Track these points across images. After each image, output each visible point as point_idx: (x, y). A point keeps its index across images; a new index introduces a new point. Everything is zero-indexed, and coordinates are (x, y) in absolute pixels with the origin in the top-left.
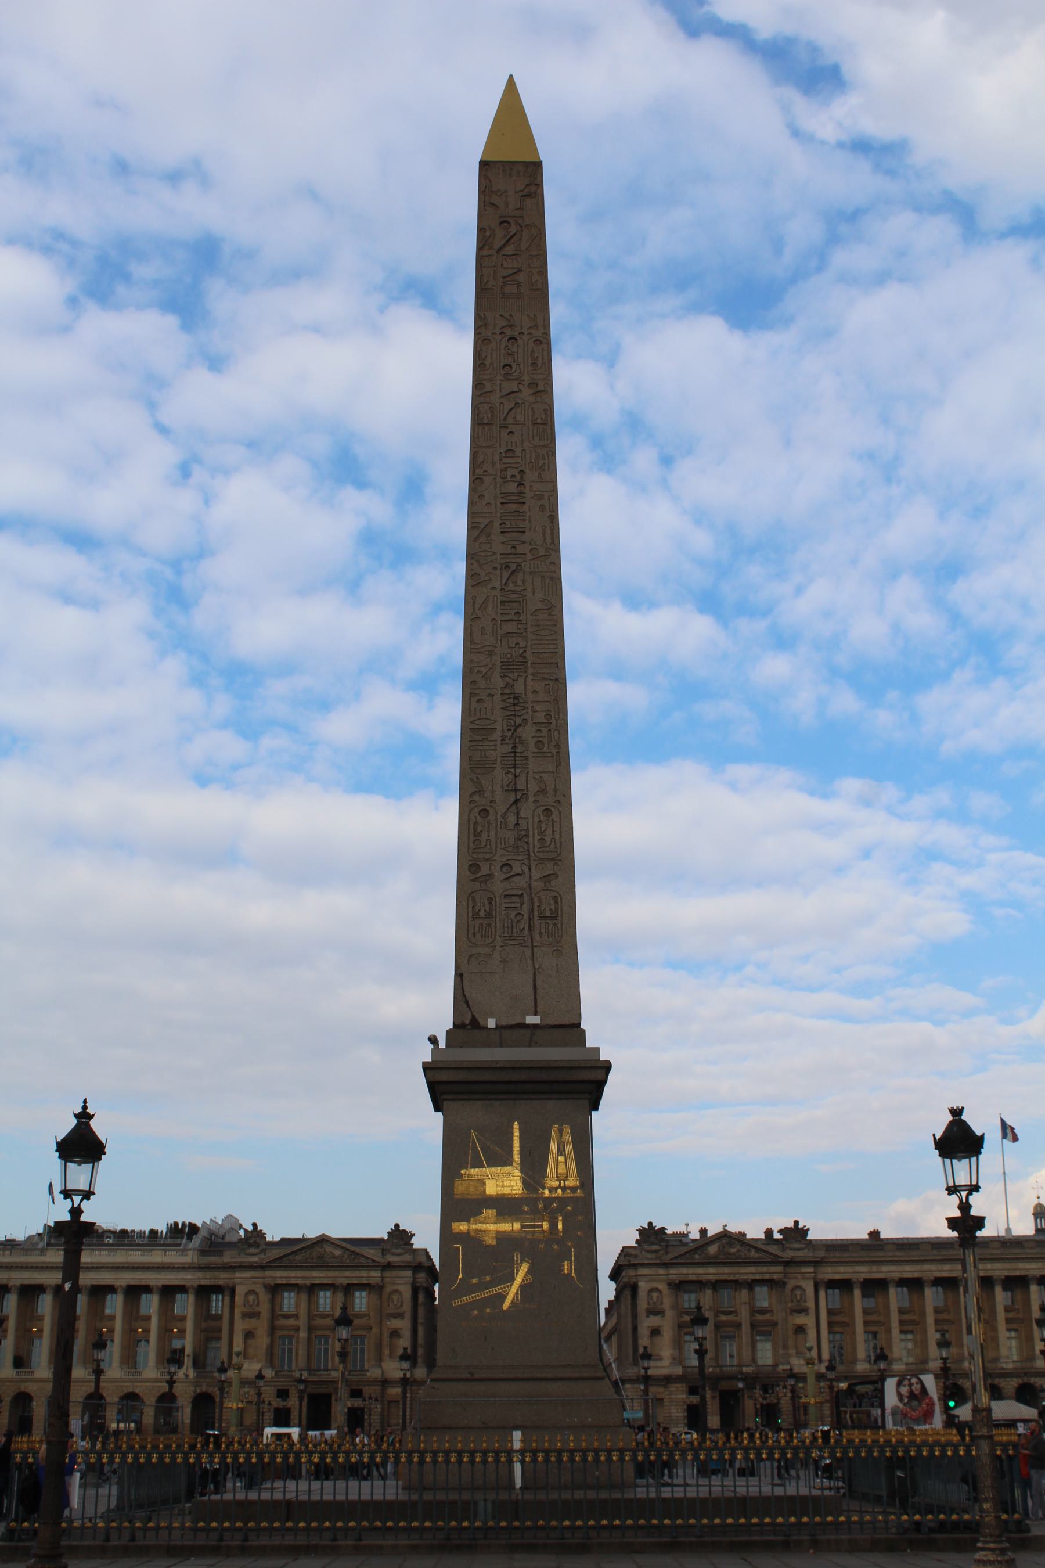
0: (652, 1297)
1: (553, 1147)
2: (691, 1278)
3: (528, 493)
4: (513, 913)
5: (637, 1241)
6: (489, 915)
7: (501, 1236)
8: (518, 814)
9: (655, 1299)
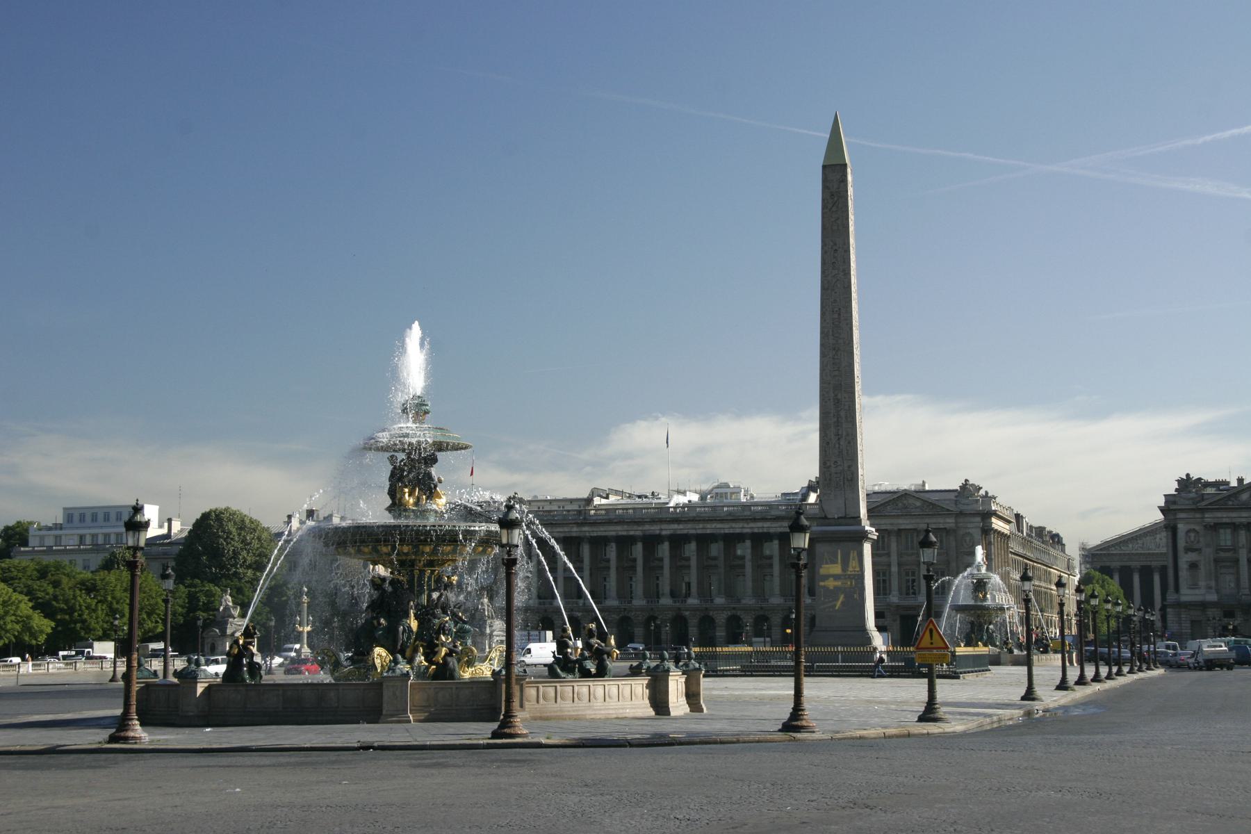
0: (1190, 537)
1: (851, 557)
2: (1224, 520)
3: (842, 318)
4: (838, 479)
5: (1176, 490)
6: (830, 480)
7: (835, 587)
8: (839, 444)
9: (1192, 539)
